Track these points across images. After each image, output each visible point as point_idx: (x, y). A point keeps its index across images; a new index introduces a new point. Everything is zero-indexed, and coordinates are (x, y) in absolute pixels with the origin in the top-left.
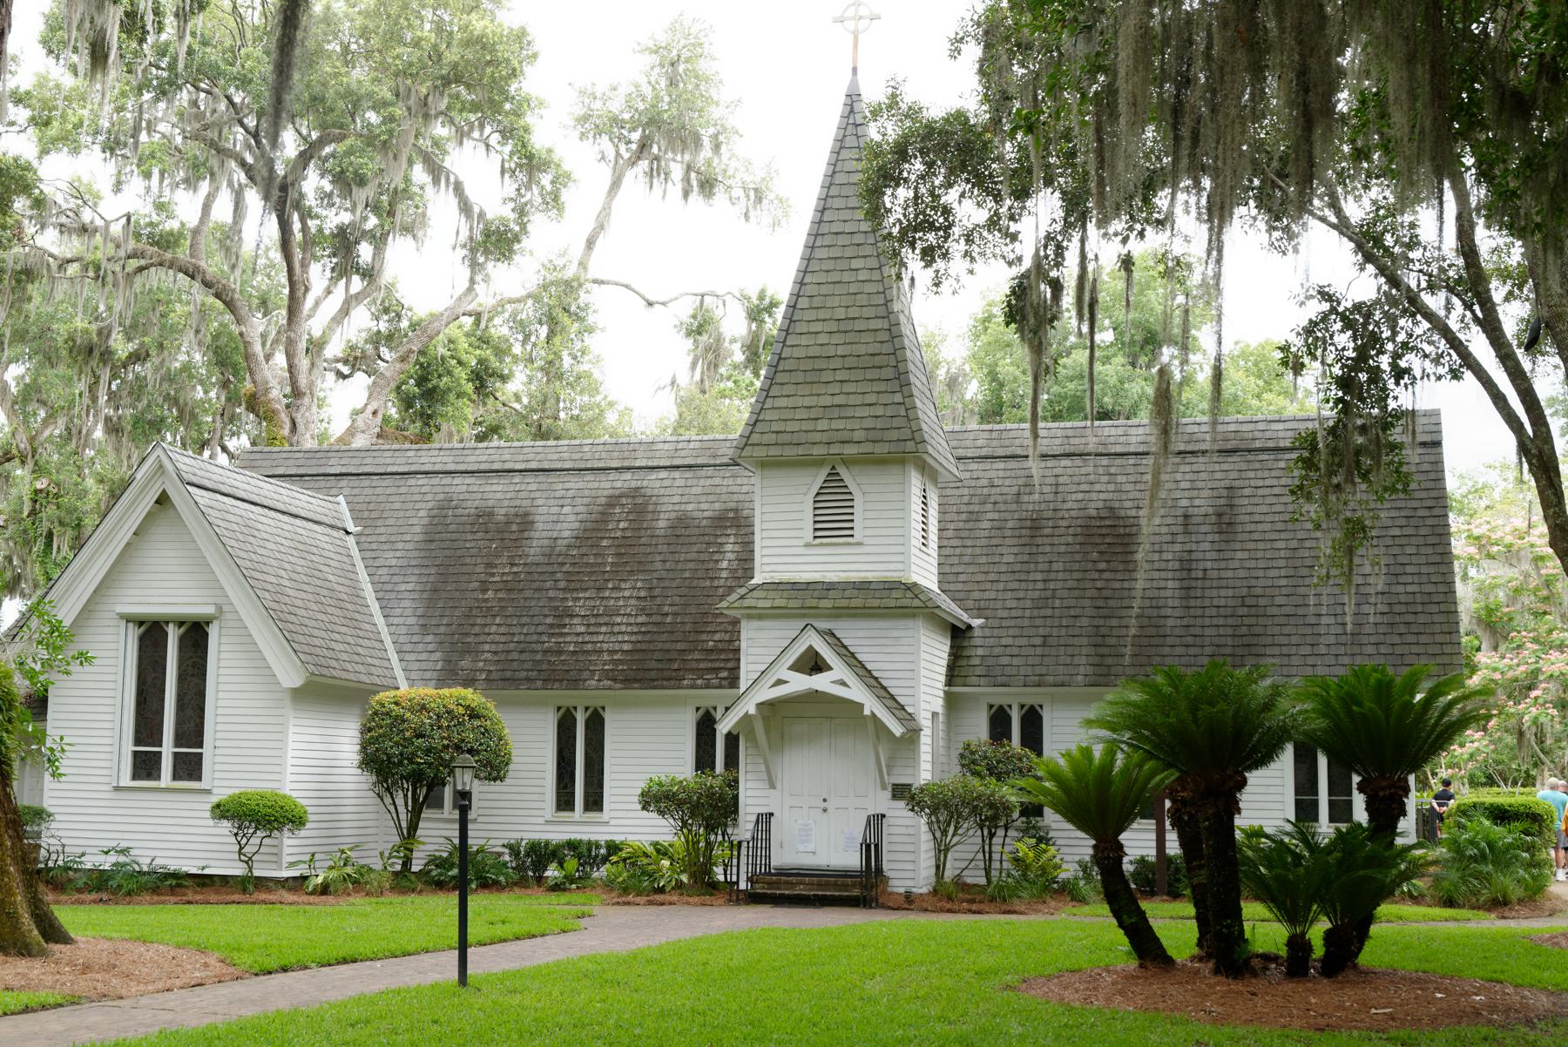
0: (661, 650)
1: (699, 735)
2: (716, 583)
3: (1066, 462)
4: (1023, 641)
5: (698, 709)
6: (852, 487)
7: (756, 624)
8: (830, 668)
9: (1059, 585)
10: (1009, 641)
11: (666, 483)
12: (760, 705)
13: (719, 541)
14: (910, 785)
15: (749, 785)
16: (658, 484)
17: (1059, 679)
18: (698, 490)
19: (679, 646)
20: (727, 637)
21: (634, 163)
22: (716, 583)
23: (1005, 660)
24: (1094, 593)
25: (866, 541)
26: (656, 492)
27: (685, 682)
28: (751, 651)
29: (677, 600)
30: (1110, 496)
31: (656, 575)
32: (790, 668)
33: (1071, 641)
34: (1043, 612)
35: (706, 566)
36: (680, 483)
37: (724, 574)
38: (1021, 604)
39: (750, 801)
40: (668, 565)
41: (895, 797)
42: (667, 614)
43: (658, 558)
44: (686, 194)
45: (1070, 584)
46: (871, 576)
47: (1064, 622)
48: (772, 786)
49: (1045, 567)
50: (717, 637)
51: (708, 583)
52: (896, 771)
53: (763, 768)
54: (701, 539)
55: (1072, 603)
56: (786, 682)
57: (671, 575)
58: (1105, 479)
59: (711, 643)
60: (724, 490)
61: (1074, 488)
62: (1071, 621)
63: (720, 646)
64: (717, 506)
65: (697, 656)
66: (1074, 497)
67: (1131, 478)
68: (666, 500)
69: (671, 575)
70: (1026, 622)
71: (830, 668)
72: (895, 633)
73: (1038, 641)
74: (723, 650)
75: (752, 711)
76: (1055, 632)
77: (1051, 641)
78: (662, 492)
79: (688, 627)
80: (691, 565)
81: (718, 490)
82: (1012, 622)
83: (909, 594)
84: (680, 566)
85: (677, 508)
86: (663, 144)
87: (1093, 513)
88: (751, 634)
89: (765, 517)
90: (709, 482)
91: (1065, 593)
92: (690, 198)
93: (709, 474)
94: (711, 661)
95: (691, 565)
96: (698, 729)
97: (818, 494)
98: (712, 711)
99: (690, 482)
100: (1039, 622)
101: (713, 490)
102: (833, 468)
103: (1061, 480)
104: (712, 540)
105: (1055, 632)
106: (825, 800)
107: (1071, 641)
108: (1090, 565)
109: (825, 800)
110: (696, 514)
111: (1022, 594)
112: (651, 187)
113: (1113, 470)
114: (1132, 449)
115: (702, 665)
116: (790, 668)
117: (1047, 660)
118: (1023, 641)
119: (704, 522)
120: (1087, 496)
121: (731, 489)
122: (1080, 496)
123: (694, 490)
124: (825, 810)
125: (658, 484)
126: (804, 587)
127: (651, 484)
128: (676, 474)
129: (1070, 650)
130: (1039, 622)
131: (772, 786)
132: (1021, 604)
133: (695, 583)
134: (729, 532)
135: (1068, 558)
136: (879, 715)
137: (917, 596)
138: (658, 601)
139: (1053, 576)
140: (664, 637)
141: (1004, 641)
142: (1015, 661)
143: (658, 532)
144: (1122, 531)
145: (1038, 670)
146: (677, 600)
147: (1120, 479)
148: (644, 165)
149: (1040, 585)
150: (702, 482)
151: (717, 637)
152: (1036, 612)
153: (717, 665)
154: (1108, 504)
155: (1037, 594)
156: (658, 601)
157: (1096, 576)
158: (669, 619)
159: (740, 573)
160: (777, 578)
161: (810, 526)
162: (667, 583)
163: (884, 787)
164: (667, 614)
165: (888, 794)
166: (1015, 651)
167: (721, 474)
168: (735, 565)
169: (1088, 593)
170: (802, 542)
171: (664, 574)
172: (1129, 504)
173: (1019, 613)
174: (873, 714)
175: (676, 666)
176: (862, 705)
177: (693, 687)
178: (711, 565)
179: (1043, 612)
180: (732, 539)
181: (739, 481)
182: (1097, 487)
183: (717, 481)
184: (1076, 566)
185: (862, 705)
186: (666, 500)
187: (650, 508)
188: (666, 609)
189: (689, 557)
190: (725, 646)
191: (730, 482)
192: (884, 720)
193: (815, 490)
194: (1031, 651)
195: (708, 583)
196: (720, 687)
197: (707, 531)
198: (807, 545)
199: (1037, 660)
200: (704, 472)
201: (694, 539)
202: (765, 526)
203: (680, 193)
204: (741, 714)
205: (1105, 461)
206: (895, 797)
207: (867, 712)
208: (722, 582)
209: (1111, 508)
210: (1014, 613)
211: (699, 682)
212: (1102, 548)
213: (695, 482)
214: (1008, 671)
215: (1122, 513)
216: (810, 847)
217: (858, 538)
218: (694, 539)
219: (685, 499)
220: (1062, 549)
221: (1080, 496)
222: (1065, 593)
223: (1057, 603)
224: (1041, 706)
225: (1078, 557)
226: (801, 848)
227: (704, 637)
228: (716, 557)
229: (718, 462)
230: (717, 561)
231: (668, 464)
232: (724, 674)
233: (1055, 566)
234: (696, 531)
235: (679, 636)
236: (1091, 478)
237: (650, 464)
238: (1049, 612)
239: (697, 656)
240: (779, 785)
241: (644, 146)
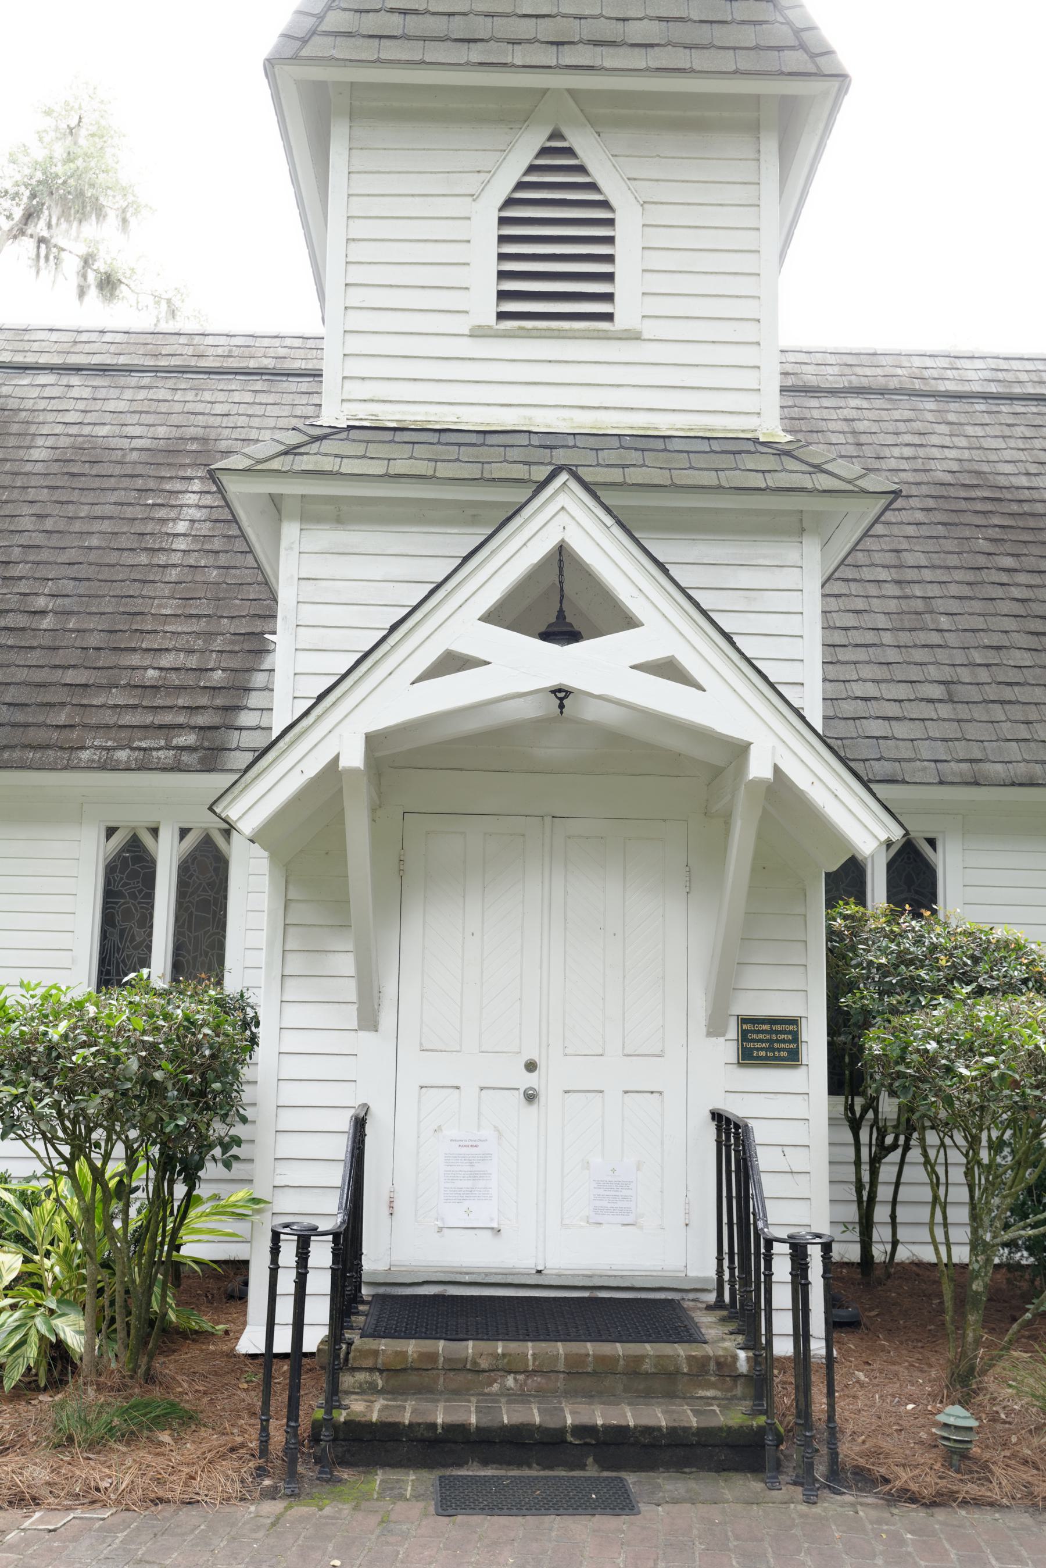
0: (27, 684)
1: (110, 896)
2: (162, 559)
3: (855, 402)
4: (902, 691)
5: (111, 832)
6: (611, 187)
7: (325, 537)
8: (628, 622)
9: (934, 591)
10: (871, 690)
11: (48, 392)
12: (373, 741)
13: (168, 487)
14: (794, 1021)
15: (294, 1015)
16: (35, 393)
17: (1021, 770)
18: (122, 406)
19: (71, 677)
20: (193, 662)
21: (15, 237)
22: (162, 559)
23: (876, 728)
24: (1017, 608)
25: (650, 329)
26: (29, 404)
27: (85, 755)
28: (308, 614)
29: (69, 586)
30: (966, 455)
31: (23, 540)
32: (492, 617)
33: (1008, 693)
34: (922, 637)
35: (139, 528)
36: (86, 393)
37: (181, 544)
38: (867, 620)
39: (292, 1067)
40: (49, 524)
41: (747, 1057)
42: (43, 613)
43: (26, 510)
44: (82, 292)
45: (954, 590)
46: (664, 424)
47: (978, 657)
48: (369, 1021)
49: (890, 558)
50: (167, 660)
51: (143, 559)
52: (752, 978)
53: (345, 964)
54: (126, 482)
55: (979, 623)
56: (489, 663)
57: (55, 540)
58: (943, 429)
59: (151, 673)
60: (178, 408)
61: (890, 439)
62: (992, 657)
63: (174, 678)
64: (162, 431)
65: (117, 698)
66: (896, 451)
67: (996, 431)
68: (51, 417)
69: (55, 540)
70: (892, 655)
71: (628, 622)
72: (745, 578)
73: (937, 692)
74: (181, 688)
75: (354, 758)
76: (965, 674)
77: (962, 692)
78: (42, 404)
79: (93, 640)
80: (106, 526)
81: (163, 408)
82: (861, 655)
83: (791, 464)
84: (77, 526)
85: (74, 430)
86: (56, 212)
87: (948, 478)
88: (312, 567)
89: (358, 252)
90: (142, 394)
91: (954, 606)
92: (86, 298)
93: (145, 381)
94: (155, 708)
95: (106, 526)
96: (108, 882)
97: (510, 202)
98: (147, 839)
99: (102, 393)
100: (919, 655)
101: (154, 406)
102: (556, 135)
103: (860, 426)
104: (152, 484)
105: (965, 674)
106: (531, 1066)
107: (1008, 693)
108: (982, 560)
109: (531, 1066)
110: (114, 443)
111: (860, 604)
112: (38, 273)
113: (951, 417)
114: (976, 388)
115: (128, 719)
116: (494, 616)
117: (972, 731)
118: (902, 691)
119: (134, 456)
120: (921, 452)
121: (189, 407)
122: (908, 452)
123: (111, 406)
124: (531, 1097)
125: (35, 393)
126: (473, 439)
127: (19, 392)
128: (75, 380)
129: (1017, 712)
130: (919, 655)
131: (369, 1021)
132: (867, 620)
133: (113, 558)
134: (189, 473)
135: (931, 545)
136: (799, 777)
137: (819, 468)
138: (23, 587)
139: (911, 574)
140: (33, 658)
141: (858, 689)
142: (900, 730)
143: (28, 468)
144: (1015, 508)
145: (961, 750)
146: (69, 586)
147: (970, 430)
148: (27, 245)
149: (891, 590)
150: (128, 394)
151: (167, 660)
152: (905, 638)
153: (168, 718)
154: (967, 466)
155: (892, 605)
156: (23, 587)
157: (1004, 578)
158: (47, 622)
159: (217, 544)
160: (390, 415)
161: (491, 286)
162: (45, 555)
163: (714, 1030)
164: (43, 613)
165: (727, 1048)
166: (893, 710)
167: (170, 384)
168: (205, 529)
169: (1006, 607)
170: (462, 324)
171: (39, 539)
172: (1008, 468)
173: (870, 637)
174: (777, 769)
175: (62, 719)
176: (740, 750)
177: (107, 766)
178: (149, 528)
179: (922, 637)
180: (196, 486)
181: (207, 396)
182: (935, 440)
183: (162, 394)
184: (953, 560)
185: (740, 750)
186: (51, 417)
187: (15, 428)
188: (41, 602)
189: (98, 510)
190: (189, 680)
191: (190, 396)
192: (819, 796)
193: (503, 186)
194: (927, 711)
195: (143, 559)
196: (177, 768)
197: (139, 469)
198: (478, 333)
199: (951, 730)
200: (133, 380)
201: (112, 483)
202: (357, 275)
203: (74, 292)
204: (313, 767)
205: (930, 405)
206: (747, 1057)
207: (759, 768)
208: (176, 558)
209: (978, 473)
210: (857, 637)
211: (122, 755)
212: (991, 533)
213: (113, 393)
214: (889, 749)
215: (1002, 481)
216: (485, 1213)
217: (622, 322)
218: (112, 483)
219: (89, 418)
220: (911, 530)
221: (908, 452)
222: (954, 606)
223: (944, 622)
224: (932, 842)
225: (949, 545)
226: (455, 1215)
227: (135, 659)
228: (162, 513)
229: (163, 362)
230: (164, 521)
231: (57, 360)
232: (188, 739)
233: (909, 559)
234: (118, 470)
235: (73, 657)
236: (917, 426)
237: (19, 359)
238: (935, 638)
239: (117, 698)
240: (387, 1019)
241: (29, 216)
